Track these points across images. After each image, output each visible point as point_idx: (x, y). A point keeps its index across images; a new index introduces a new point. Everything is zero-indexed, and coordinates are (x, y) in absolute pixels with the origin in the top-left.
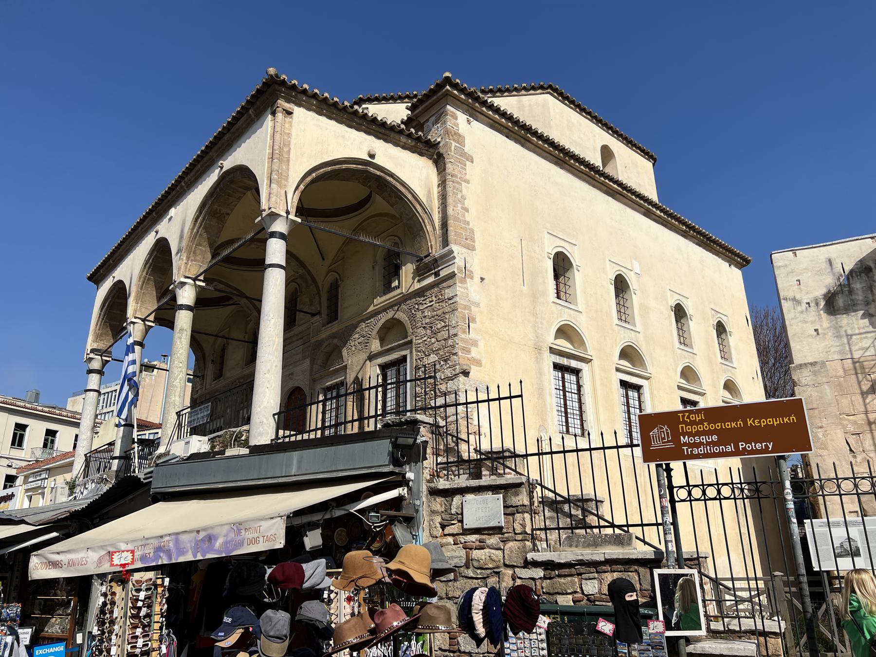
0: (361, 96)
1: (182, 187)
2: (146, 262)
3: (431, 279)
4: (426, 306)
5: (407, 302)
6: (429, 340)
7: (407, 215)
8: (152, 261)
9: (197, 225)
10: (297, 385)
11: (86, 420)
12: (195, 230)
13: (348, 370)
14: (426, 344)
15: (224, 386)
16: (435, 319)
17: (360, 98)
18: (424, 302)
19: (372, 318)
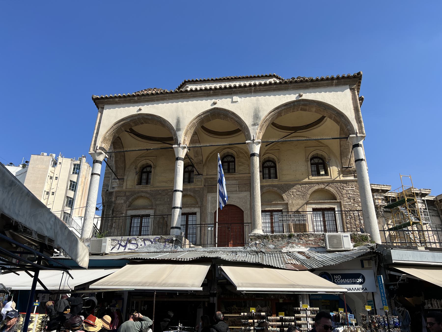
0: (275, 74)
1: (251, 89)
2: (199, 116)
3: (352, 178)
4: (349, 189)
5: (335, 184)
6: (353, 204)
7: (345, 147)
8: (203, 117)
9: (269, 115)
11: (95, 194)
12: (267, 117)
13: (289, 206)
14: (351, 206)
15: (150, 190)
16: (357, 196)
17: (274, 75)
18: (347, 187)
19: (307, 184)
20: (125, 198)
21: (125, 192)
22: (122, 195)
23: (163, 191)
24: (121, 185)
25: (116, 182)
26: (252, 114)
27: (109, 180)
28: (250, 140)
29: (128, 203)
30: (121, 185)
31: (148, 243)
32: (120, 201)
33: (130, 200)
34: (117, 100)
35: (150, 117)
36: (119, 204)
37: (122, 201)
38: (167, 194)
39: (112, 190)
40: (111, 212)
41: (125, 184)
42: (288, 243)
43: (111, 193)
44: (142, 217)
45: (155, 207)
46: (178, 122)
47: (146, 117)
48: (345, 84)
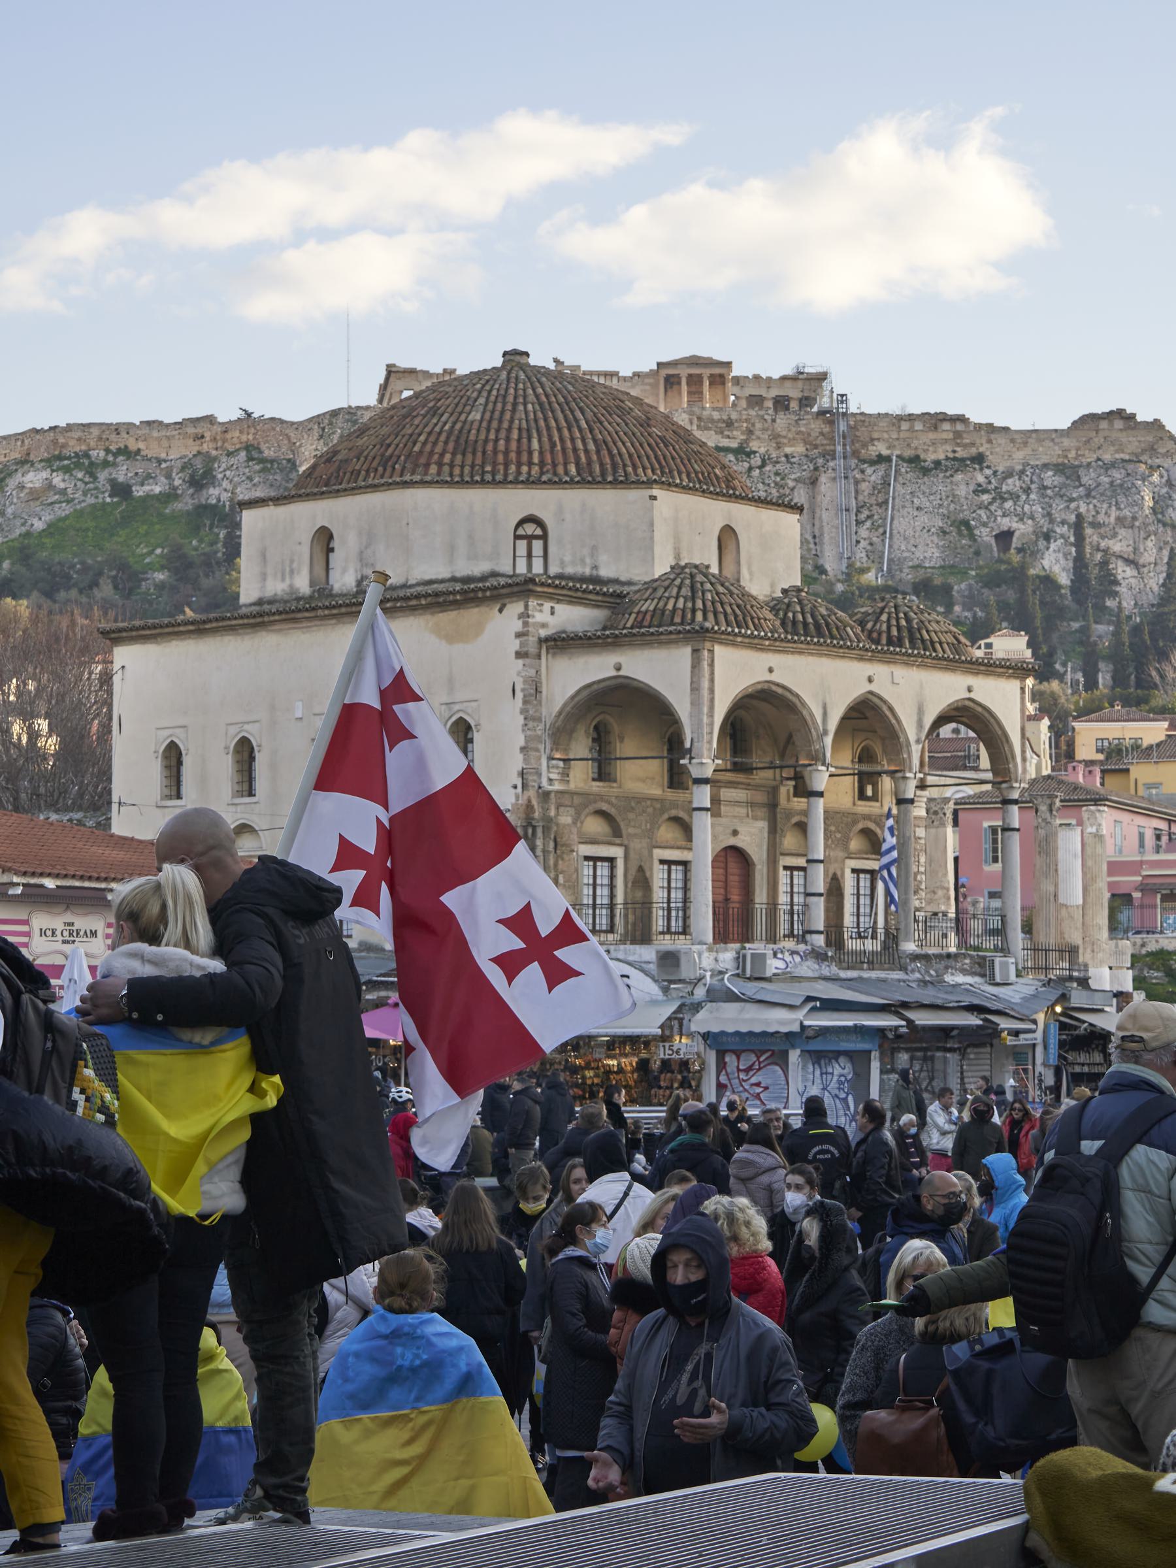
10: (740, 844)
20: (572, 811)
21: (572, 794)
22: (567, 803)
23: (639, 802)
24: (565, 774)
25: (557, 767)
26: (915, 718)
27: (539, 758)
28: (910, 771)
29: (579, 824)
30: (565, 774)
31: (797, 959)
32: (566, 819)
33: (583, 817)
34: (739, 639)
35: (780, 691)
36: (564, 826)
37: (569, 820)
38: (644, 812)
39: (550, 788)
40: (552, 844)
41: (571, 775)
42: (947, 968)
43: (545, 796)
44: (595, 859)
45: (626, 842)
46: (825, 714)
47: (774, 688)
48: (1017, 678)
